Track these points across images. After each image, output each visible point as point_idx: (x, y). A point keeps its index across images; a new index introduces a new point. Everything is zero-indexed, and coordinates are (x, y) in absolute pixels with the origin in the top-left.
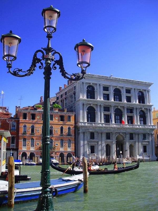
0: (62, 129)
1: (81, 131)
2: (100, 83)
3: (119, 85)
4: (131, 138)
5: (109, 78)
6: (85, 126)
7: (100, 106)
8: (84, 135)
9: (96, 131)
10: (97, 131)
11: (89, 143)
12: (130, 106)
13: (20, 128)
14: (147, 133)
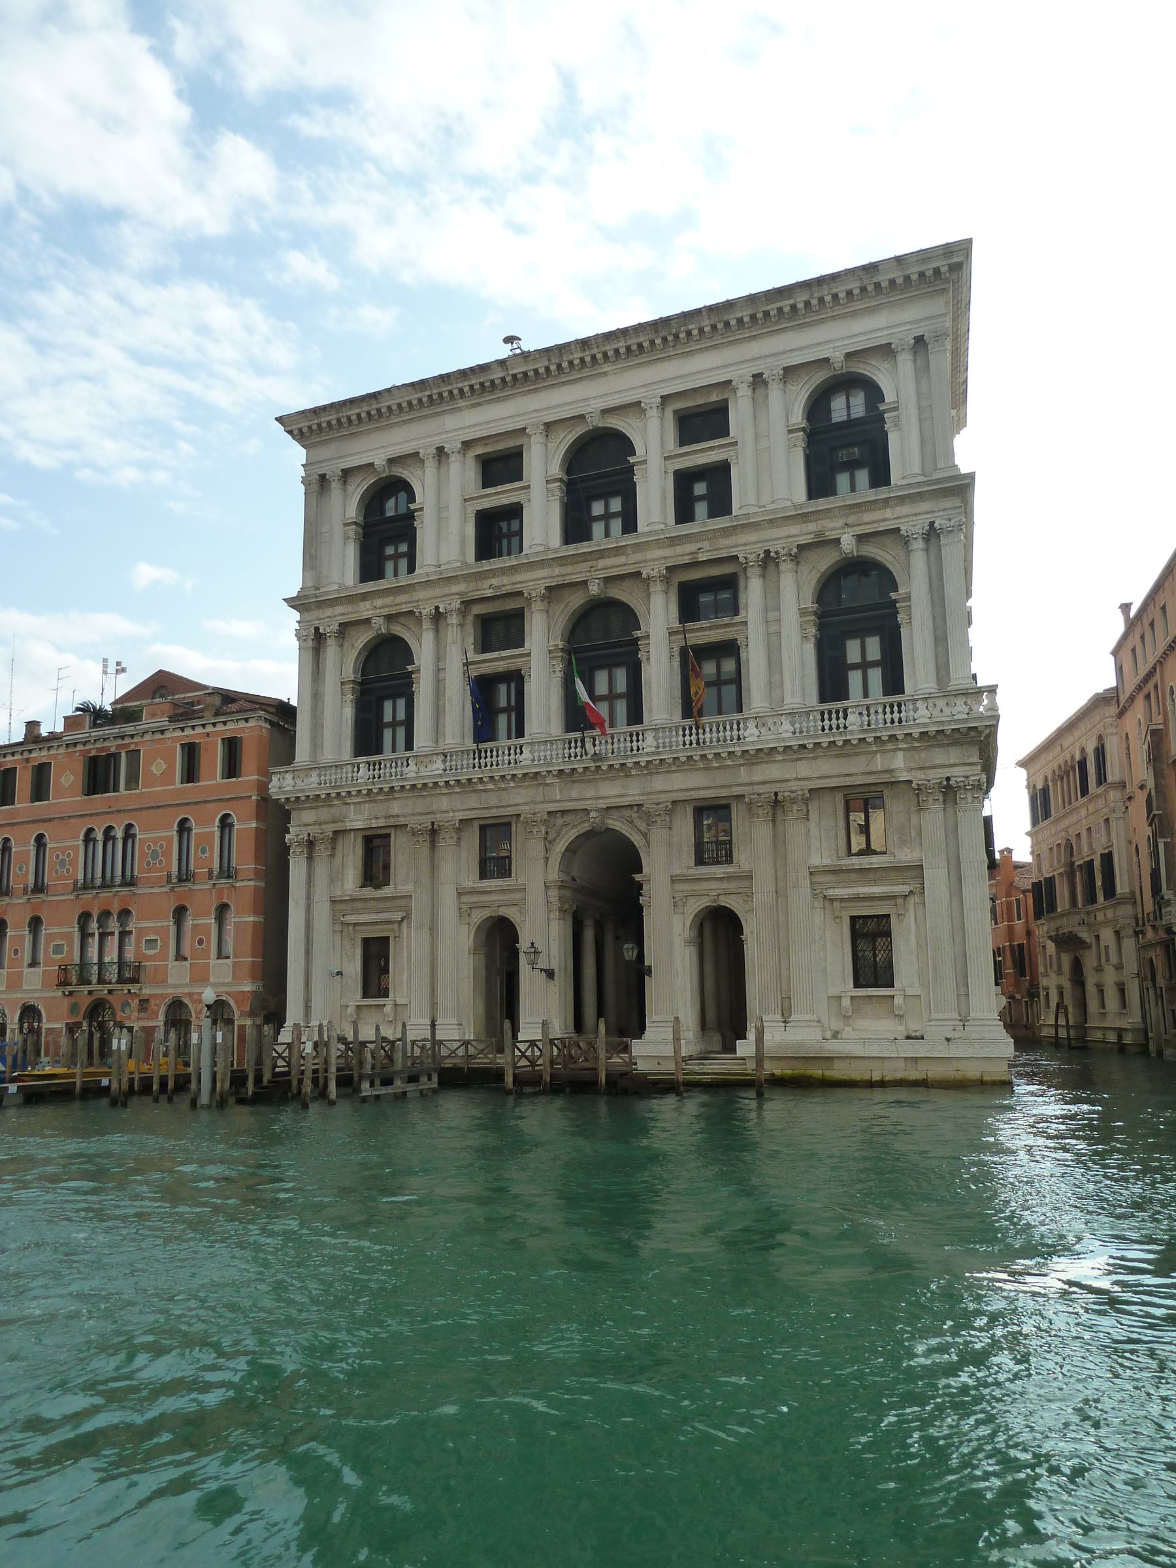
0: (183, 827)
2: (438, 441)
3: (587, 398)
4: (712, 851)
5: (497, 375)
7: (438, 617)
9: (392, 822)
10: (402, 821)
12: (702, 557)
14: (884, 778)
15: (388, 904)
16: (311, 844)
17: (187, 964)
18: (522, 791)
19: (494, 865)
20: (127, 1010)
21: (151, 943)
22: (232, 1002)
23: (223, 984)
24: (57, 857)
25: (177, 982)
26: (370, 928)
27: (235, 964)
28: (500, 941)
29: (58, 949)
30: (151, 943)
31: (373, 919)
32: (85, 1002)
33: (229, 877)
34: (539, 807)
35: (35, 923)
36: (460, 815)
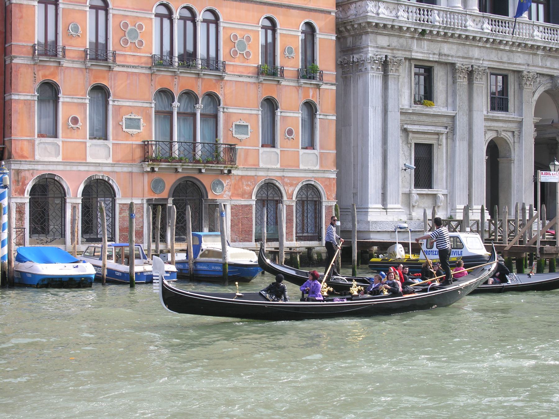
1: (370, 55)
6: (393, 26)
8: (385, 77)
9: (443, 59)
10: (450, 60)
11: (409, 127)
13: (15, 12)
15: (435, 120)
16: (385, 64)
17: (277, 150)
18: (521, 55)
19: (499, 102)
20: (218, 189)
21: (242, 128)
22: (320, 187)
23: (313, 171)
24: (126, 25)
25: (269, 166)
26: (422, 136)
27: (321, 154)
28: (495, 153)
29: (133, 123)
30: (242, 128)
31: (424, 131)
32: (170, 181)
33: (217, 69)
34: (531, 69)
35: (101, 92)
36: (486, 64)
